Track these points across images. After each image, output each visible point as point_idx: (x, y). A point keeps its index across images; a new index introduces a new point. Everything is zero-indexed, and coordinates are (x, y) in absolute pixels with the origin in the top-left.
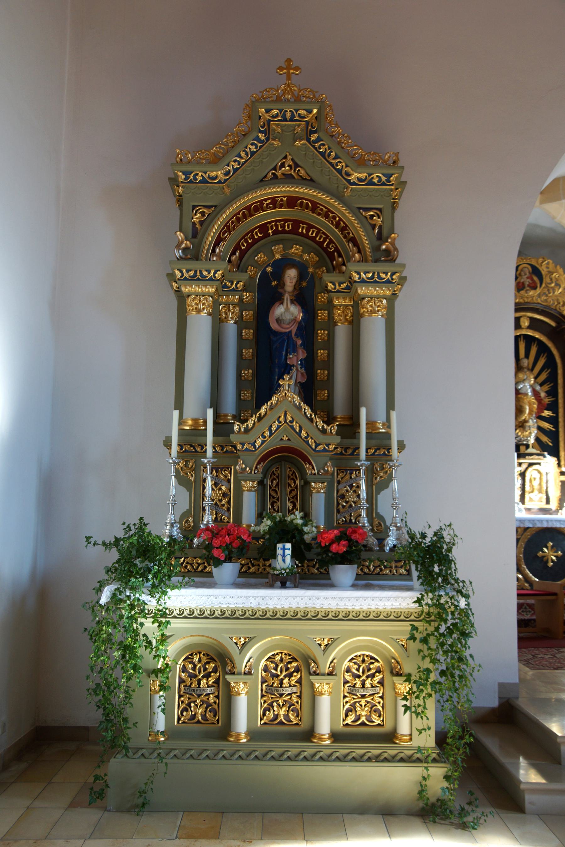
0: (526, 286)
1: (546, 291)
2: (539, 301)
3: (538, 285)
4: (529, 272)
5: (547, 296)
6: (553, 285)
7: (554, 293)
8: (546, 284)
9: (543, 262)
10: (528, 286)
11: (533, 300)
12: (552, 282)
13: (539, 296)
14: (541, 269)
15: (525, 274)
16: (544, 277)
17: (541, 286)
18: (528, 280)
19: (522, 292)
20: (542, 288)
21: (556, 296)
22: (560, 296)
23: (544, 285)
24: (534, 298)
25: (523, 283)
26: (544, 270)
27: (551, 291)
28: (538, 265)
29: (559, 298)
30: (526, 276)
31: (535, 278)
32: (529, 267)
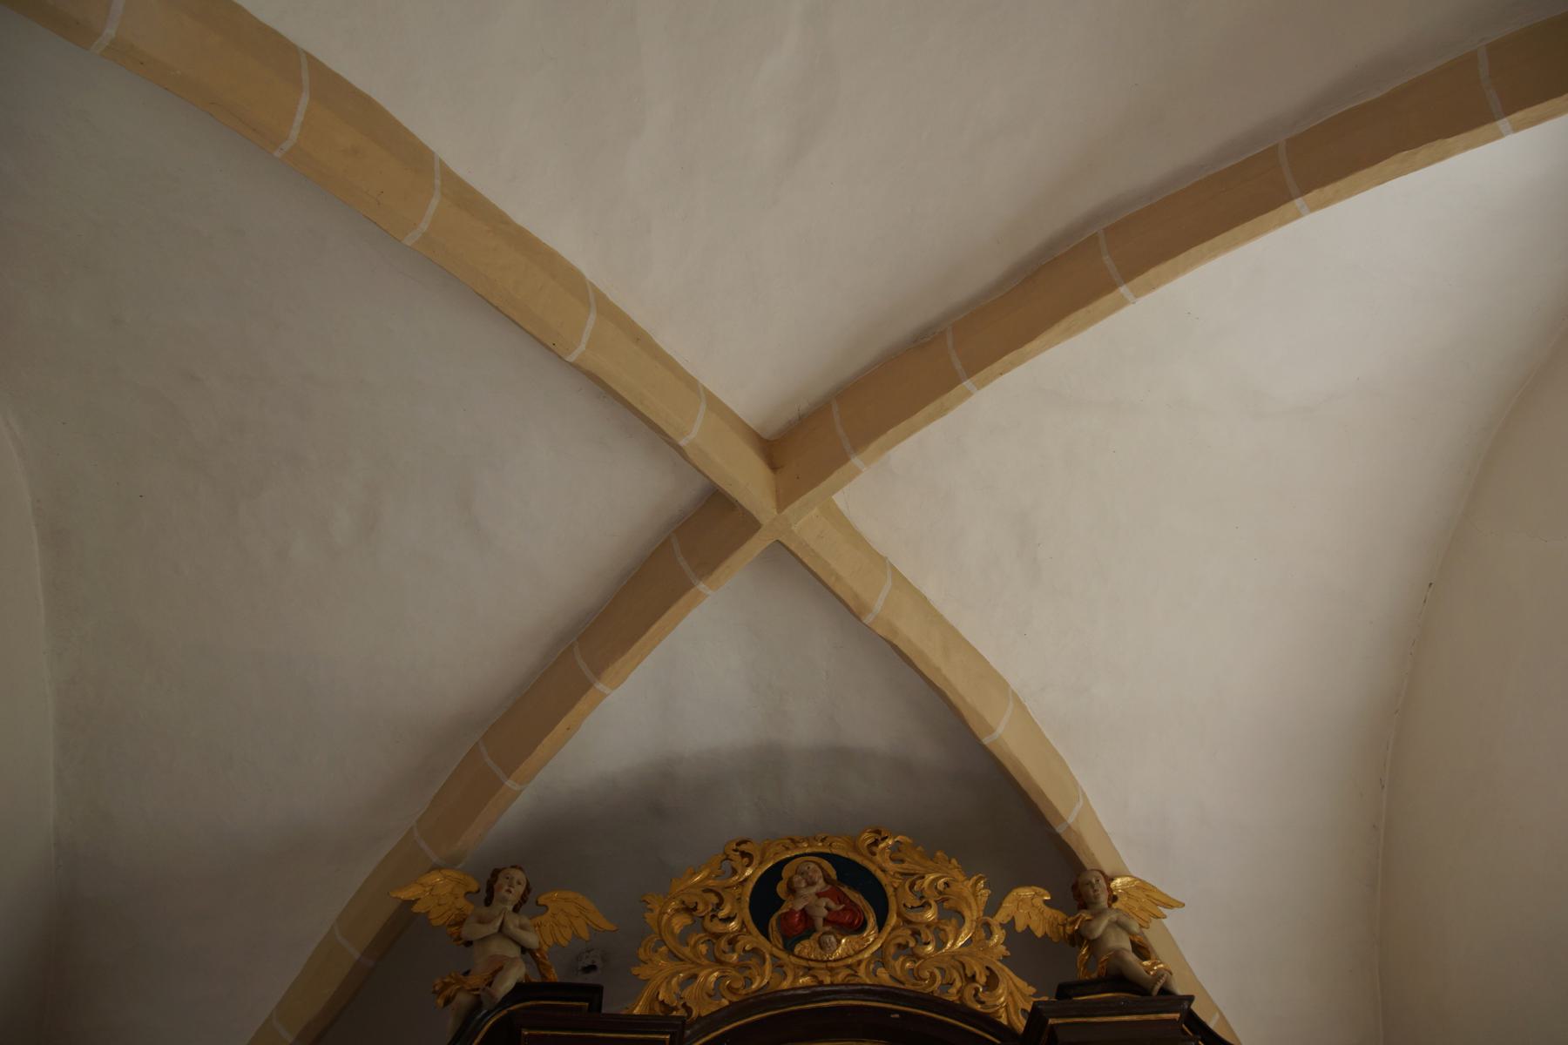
0: (820, 922)
1: (905, 935)
2: (884, 976)
3: (872, 921)
4: (827, 879)
5: (915, 956)
6: (930, 915)
7: (941, 944)
8: (899, 915)
9: (876, 843)
10: (826, 921)
11: (855, 975)
12: (925, 906)
13: (880, 958)
14: (872, 868)
15: (811, 884)
16: (890, 891)
17: (881, 924)
18: (824, 902)
19: (806, 947)
20: (888, 929)
21: (953, 956)
22: (971, 955)
23: (893, 920)
24: (862, 970)
25: (805, 914)
26: (883, 866)
27: (927, 935)
28: (861, 854)
29: (966, 959)
30: (814, 890)
31: (856, 897)
32: (825, 864)
